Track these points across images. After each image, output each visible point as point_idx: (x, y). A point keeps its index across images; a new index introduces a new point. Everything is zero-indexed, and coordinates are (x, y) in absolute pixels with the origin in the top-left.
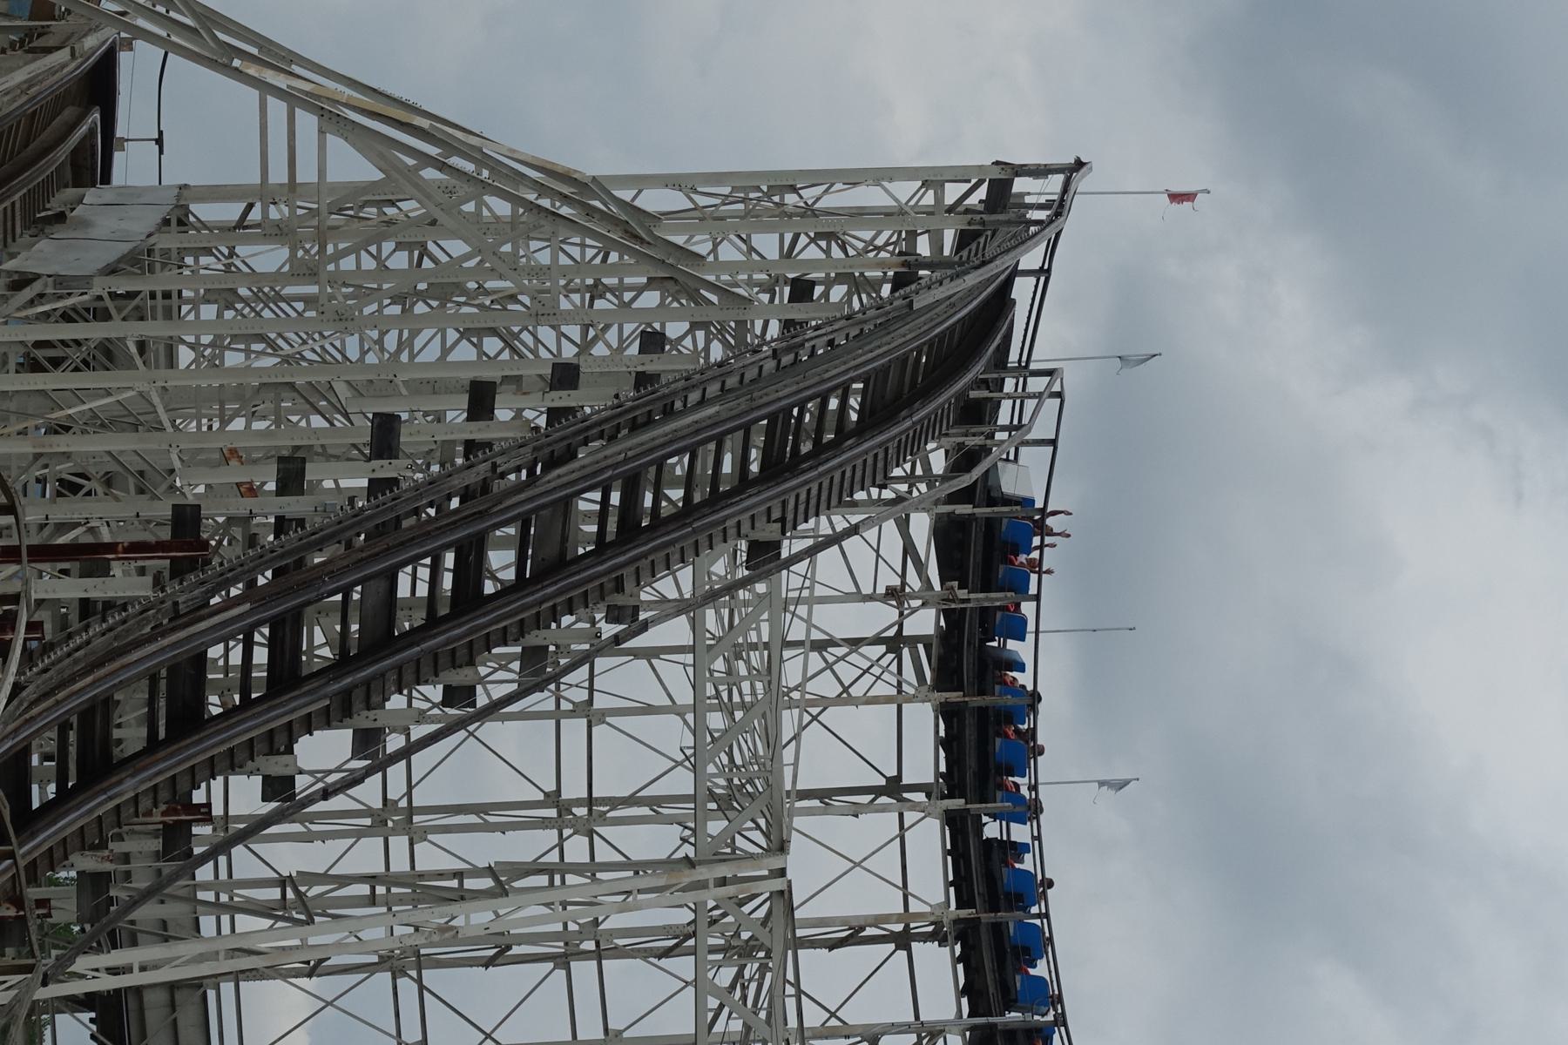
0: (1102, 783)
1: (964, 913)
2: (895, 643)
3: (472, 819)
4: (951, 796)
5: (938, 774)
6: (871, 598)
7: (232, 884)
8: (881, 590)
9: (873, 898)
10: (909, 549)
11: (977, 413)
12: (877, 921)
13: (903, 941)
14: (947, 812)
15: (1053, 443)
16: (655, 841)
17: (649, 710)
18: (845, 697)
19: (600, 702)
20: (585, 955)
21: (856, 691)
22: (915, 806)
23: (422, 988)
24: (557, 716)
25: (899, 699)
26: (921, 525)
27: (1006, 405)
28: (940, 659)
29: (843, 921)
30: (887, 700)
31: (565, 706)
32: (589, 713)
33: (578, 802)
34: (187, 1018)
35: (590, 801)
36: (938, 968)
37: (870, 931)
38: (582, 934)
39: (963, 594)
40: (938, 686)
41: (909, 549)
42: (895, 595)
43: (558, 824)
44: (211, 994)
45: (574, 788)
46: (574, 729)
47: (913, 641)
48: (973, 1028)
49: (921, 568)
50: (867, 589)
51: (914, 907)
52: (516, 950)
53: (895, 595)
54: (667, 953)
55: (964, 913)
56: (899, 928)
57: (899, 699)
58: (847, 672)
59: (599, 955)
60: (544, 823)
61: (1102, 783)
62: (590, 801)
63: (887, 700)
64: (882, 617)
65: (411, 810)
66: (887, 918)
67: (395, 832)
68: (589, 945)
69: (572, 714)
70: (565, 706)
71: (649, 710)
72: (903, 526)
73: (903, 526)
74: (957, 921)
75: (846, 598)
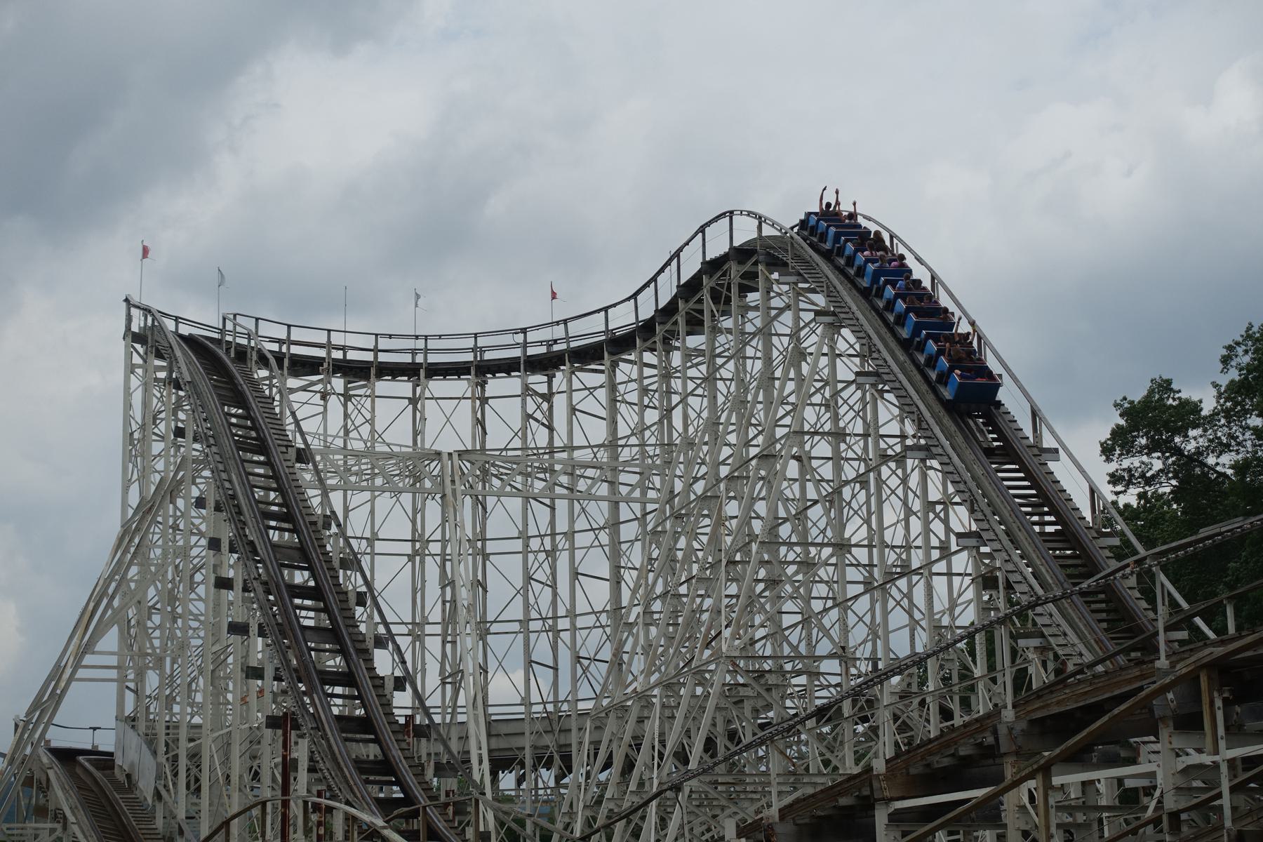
0: (416, 306)
1: (473, 372)
2: (347, 397)
3: (419, 595)
4: (419, 375)
5: (408, 381)
6: (325, 407)
7: (443, 707)
8: (322, 402)
9: (464, 414)
10: (304, 389)
11: (241, 354)
12: (474, 412)
13: (484, 400)
14: (427, 377)
15: (257, 319)
16: (433, 511)
17: (372, 512)
18: (371, 422)
19: (368, 534)
20: (484, 546)
21: (368, 416)
22: (423, 392)
23: (495, 621)
24: (373, 554)
25: (373, 397)
26: (293, 383)
27: (239, 340)
28: (355, 376)
29: (473, 428)
30: (373, 402)
31: (368, 550)
32: (371, 541)
33: (413, 546)
34: (504, 729)
35: (413, 541)
36: (497, 385)
37: (479, 416)
38: (473, 546)
39: (325, 365)
40: (367, 378)
41: (304, 389)
42: (324, 396)
43: (423, 556)
44: (494, 718)
45: (407, 548)
46: (379, 547)
47: (346, 389)
48: (526, 371)
49: (313, 384)
50: (321, 409)
51: (469, 394)
52: (480, 578)
53: (324, 396)
54: (484, 509)
55: (473, 372)
56: (478, 402)
57: (373, 397)
58: (359, 420)
59: (484, 540)
60: (422, 562)
61: (416, 306)
62: (413, 541)
63: (373, 402)
64: (334, 403)
65: (413, 623)
66: (473, 408)
67: (423, 631)
68: (479, 544)
69: (372, 547)
70: (368, 550)
71: (372, 512)
72: (292, 391)
73: (292, 391)
74: (476, 376)
75: (325, 419)
